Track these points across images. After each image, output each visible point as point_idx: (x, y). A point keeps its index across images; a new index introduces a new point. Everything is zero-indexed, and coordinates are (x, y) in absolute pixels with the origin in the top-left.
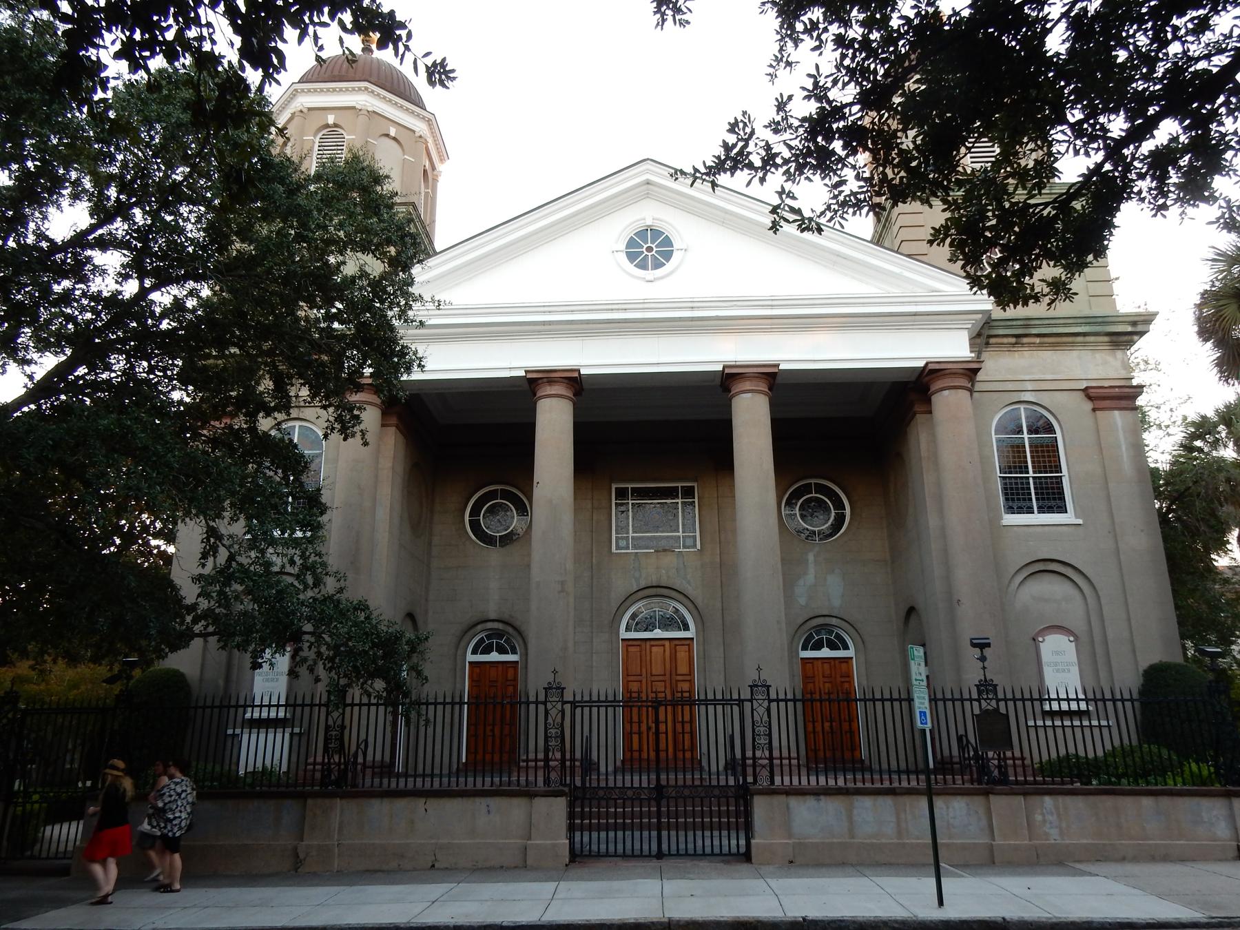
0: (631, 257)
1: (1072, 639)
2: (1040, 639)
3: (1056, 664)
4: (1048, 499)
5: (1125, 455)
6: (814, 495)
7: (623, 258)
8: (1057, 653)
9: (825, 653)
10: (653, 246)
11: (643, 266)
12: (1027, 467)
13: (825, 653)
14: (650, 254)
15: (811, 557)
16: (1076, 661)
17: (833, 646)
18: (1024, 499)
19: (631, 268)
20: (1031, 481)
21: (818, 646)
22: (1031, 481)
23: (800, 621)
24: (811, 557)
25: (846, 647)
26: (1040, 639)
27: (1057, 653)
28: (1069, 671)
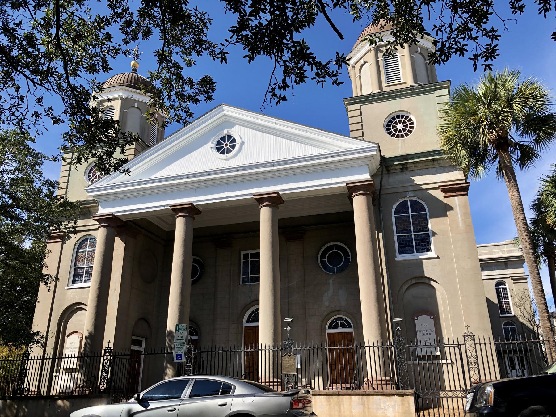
0: (218, 149)
1: (432, 317)
2: (416, 318)
3: (423, 331)
4: (422, 245)
5: (460, 219)
6: (334, 251)
7: (214, 150)
8: (424, 325)
9: (340, 330)
10: (226, 143)
11: (223, 153)
12: (411, 230)
13: (340, 330)
14: (228, 146)
15: (331, 281)
16: (434, 328)
17: (344, 326)
18: (409, 246)
19: (218, 154)
20: (413, 236)
21: (336, 327)
22: (413, 236)
23: (326, 313)
24: (331, 281)
25: (350, 327)
26: (416, 318)
27: (424, 325)
28: (430, 334)
